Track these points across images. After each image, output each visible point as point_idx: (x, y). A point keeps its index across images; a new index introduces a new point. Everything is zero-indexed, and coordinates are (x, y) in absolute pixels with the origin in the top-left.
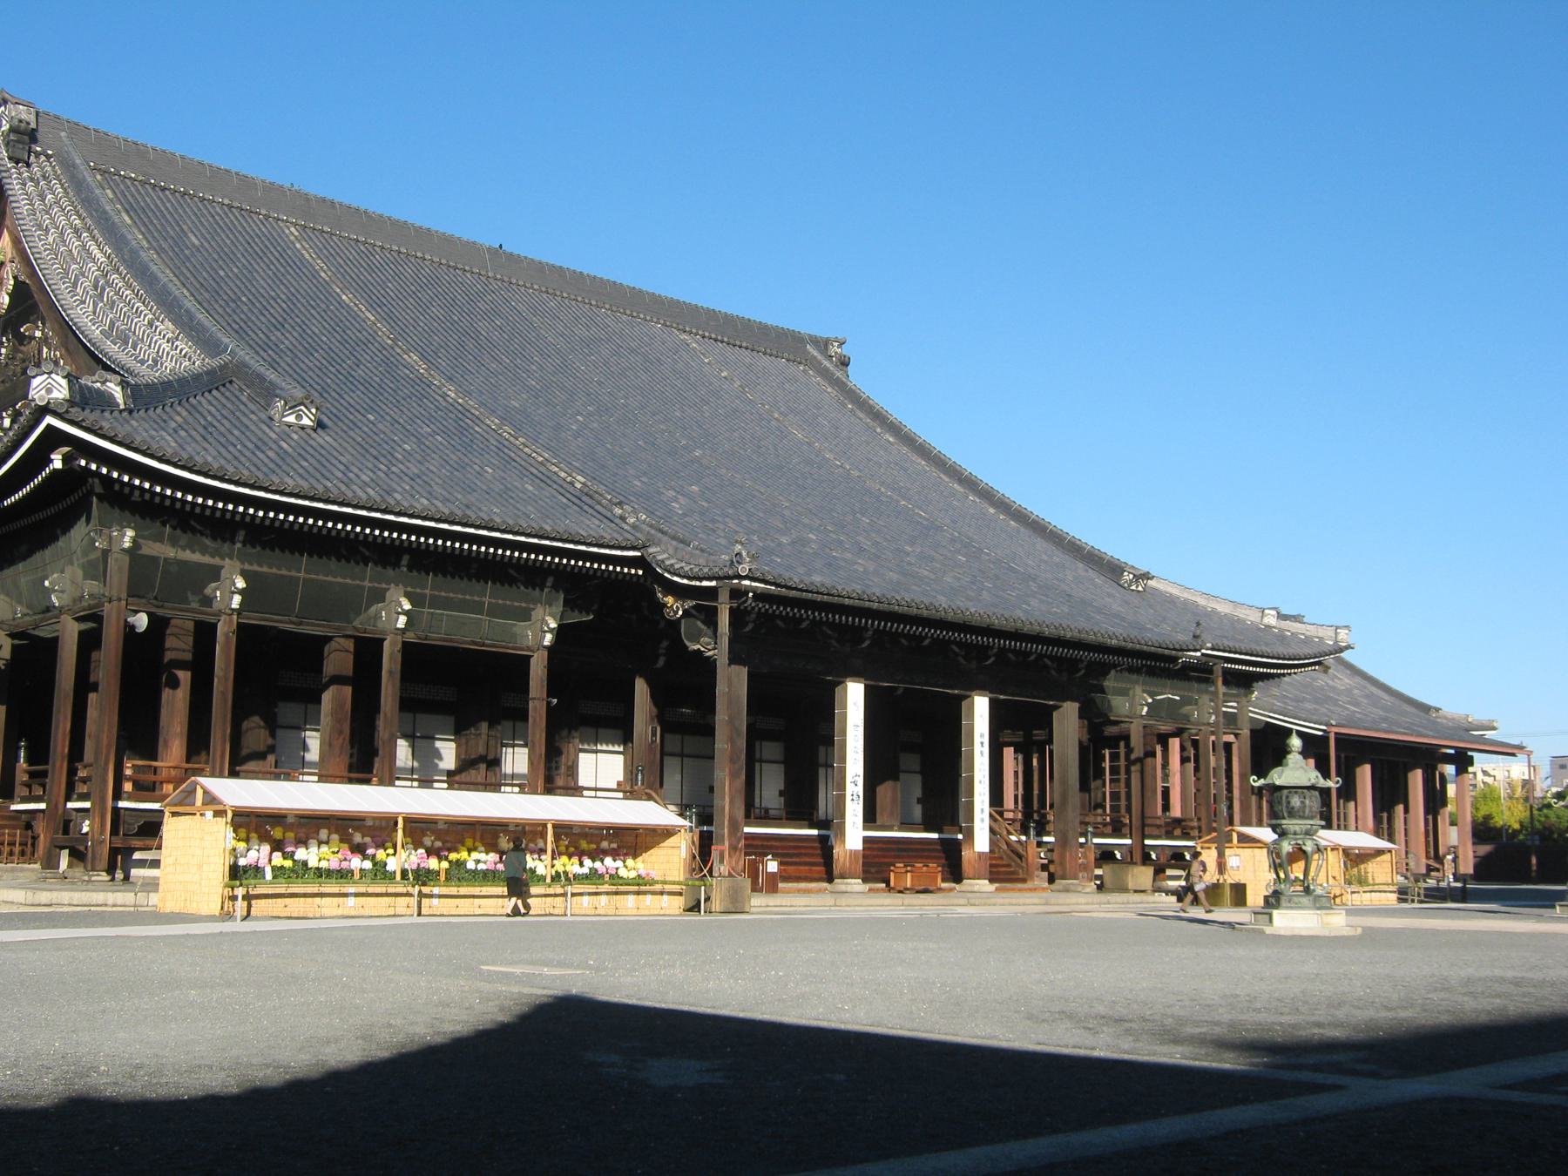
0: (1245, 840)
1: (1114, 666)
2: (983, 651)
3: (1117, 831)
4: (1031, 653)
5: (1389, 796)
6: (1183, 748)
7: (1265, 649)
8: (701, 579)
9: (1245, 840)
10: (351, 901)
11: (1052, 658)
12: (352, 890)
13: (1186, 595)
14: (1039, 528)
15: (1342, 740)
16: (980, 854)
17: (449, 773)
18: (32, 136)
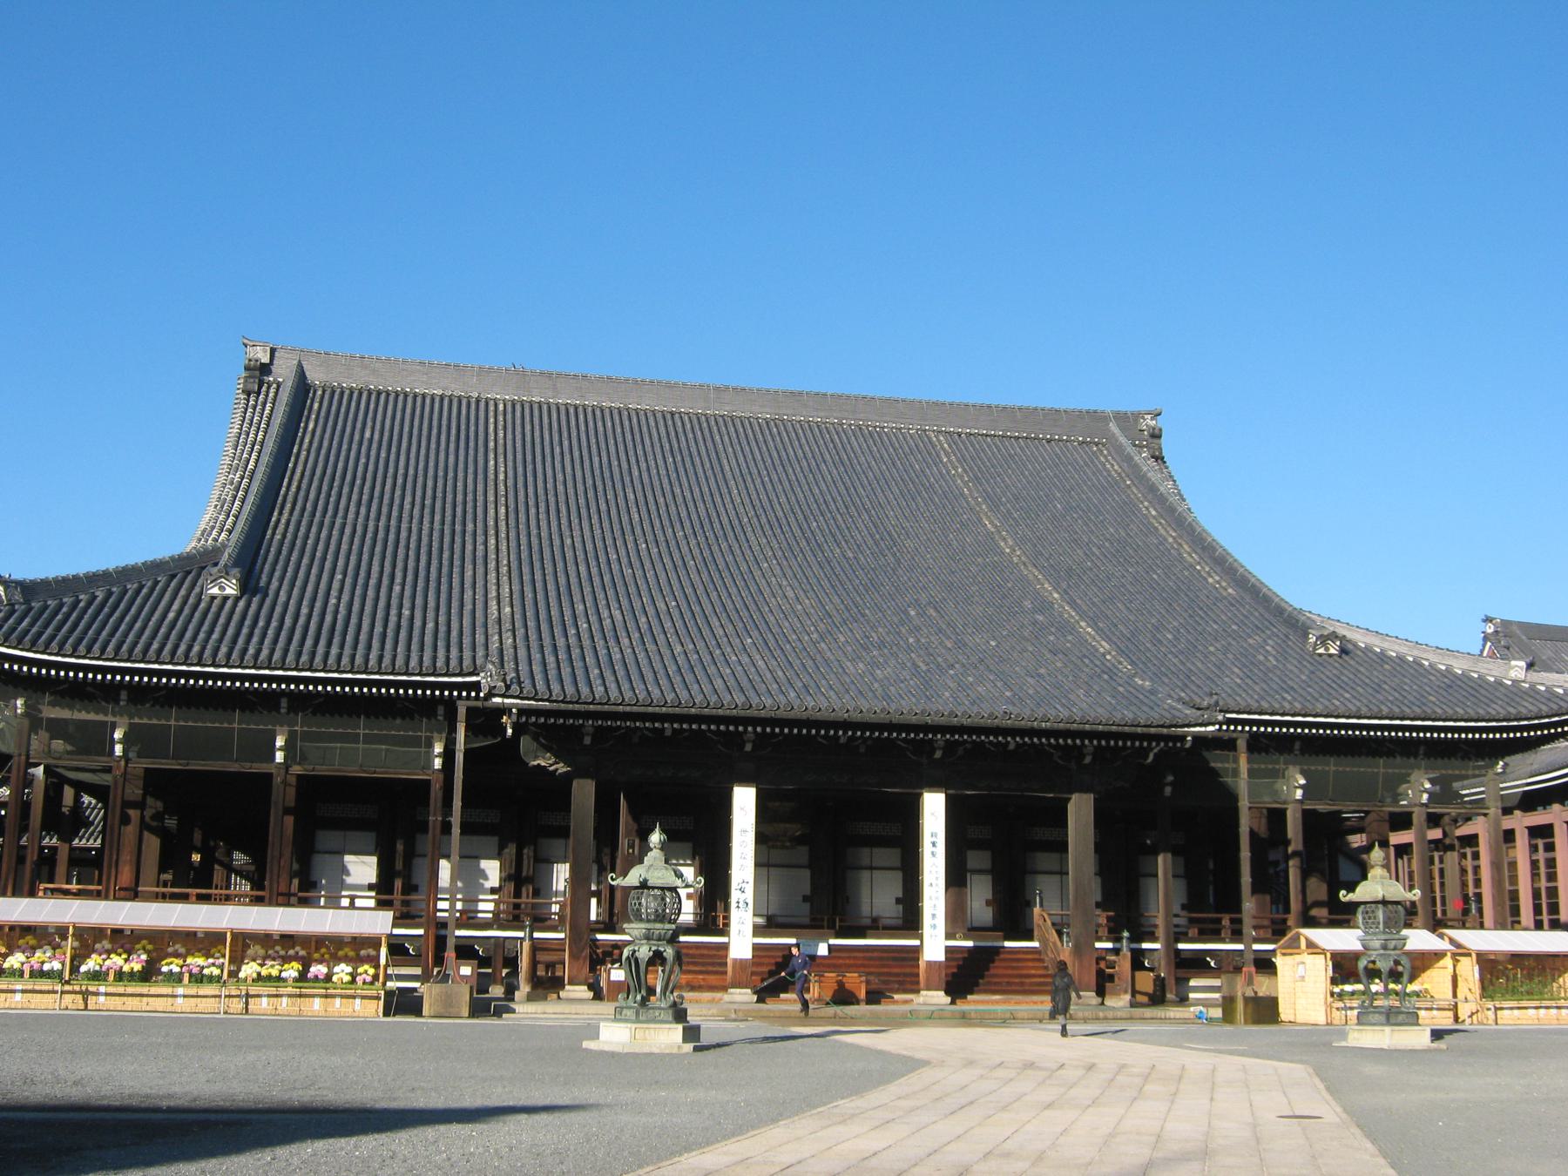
9: (1311, 945)
10: (18, 996)
12: (19, 987)
16: (929, 963)
17: (493, 891)
18: (265, 369)
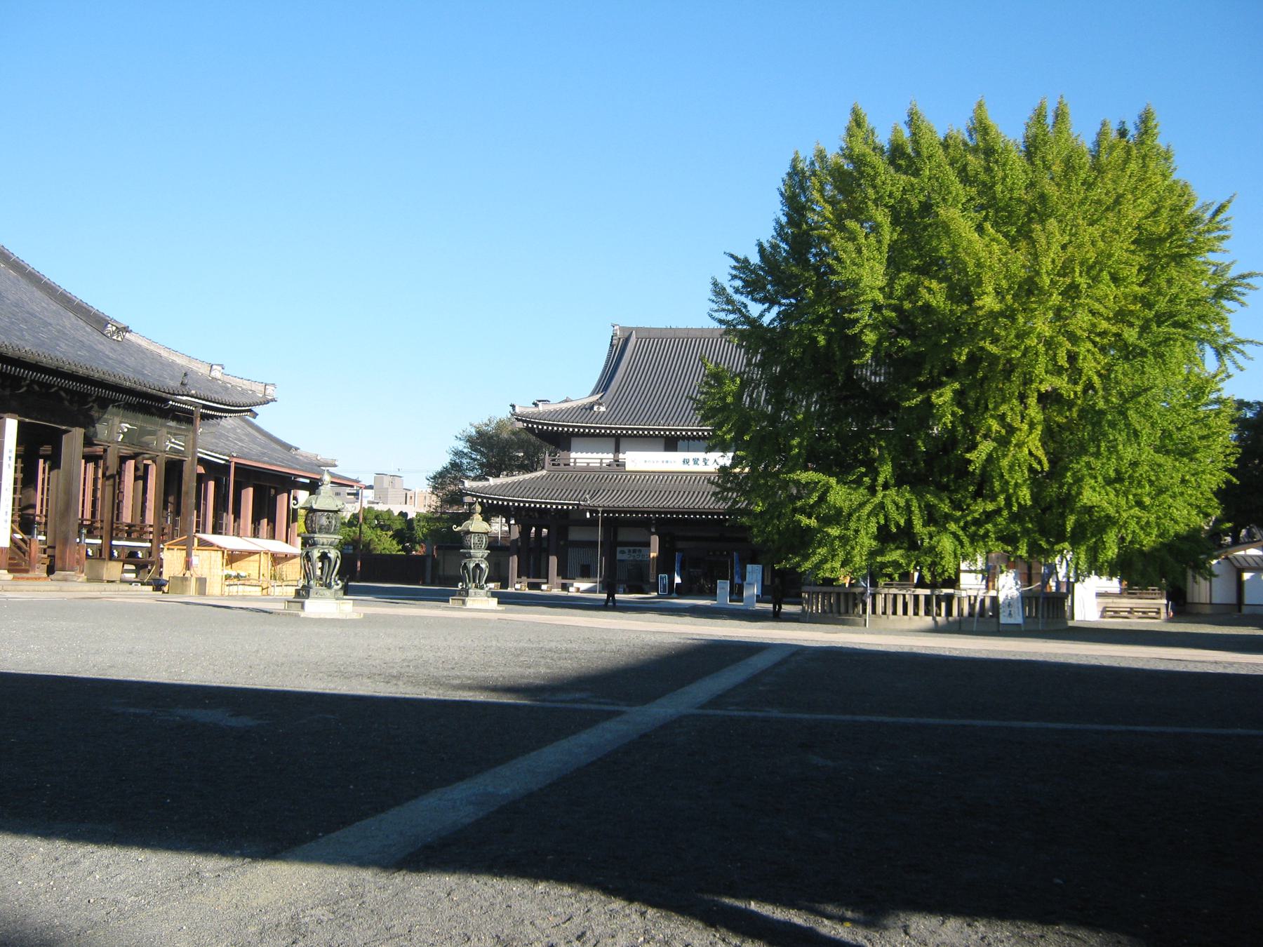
0: (203, 543)
1: (113, 401)
2: (16, 381)
3: (90, 534)
4: (53, 386)
5: (264, 510)
6: (136, 469)
7: (217, 397)
9: (203, 543)
11: (67, 391)
13: (152, 348)
14: (34, 279)
15: (241, 469)
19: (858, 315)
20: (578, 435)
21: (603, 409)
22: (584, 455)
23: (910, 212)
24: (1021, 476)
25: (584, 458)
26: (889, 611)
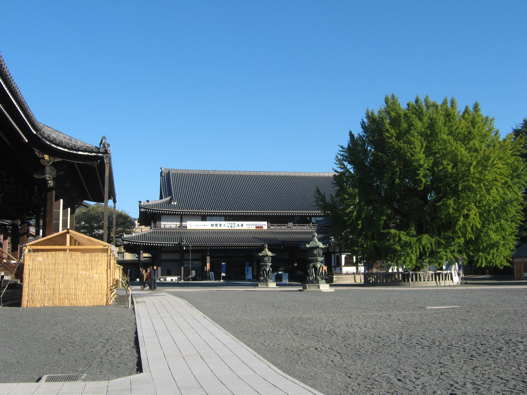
8: (78, 150)
19: (419, 172)
20: (166, 214)
21: (175, 203)
22: (168, 223)
23: (427, 135)
24: (469, 229)
25: (167, 224)
26: (418, 280)
